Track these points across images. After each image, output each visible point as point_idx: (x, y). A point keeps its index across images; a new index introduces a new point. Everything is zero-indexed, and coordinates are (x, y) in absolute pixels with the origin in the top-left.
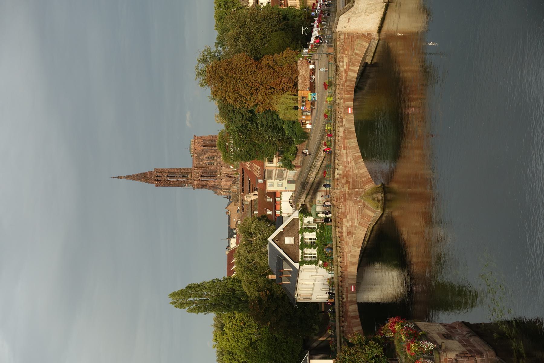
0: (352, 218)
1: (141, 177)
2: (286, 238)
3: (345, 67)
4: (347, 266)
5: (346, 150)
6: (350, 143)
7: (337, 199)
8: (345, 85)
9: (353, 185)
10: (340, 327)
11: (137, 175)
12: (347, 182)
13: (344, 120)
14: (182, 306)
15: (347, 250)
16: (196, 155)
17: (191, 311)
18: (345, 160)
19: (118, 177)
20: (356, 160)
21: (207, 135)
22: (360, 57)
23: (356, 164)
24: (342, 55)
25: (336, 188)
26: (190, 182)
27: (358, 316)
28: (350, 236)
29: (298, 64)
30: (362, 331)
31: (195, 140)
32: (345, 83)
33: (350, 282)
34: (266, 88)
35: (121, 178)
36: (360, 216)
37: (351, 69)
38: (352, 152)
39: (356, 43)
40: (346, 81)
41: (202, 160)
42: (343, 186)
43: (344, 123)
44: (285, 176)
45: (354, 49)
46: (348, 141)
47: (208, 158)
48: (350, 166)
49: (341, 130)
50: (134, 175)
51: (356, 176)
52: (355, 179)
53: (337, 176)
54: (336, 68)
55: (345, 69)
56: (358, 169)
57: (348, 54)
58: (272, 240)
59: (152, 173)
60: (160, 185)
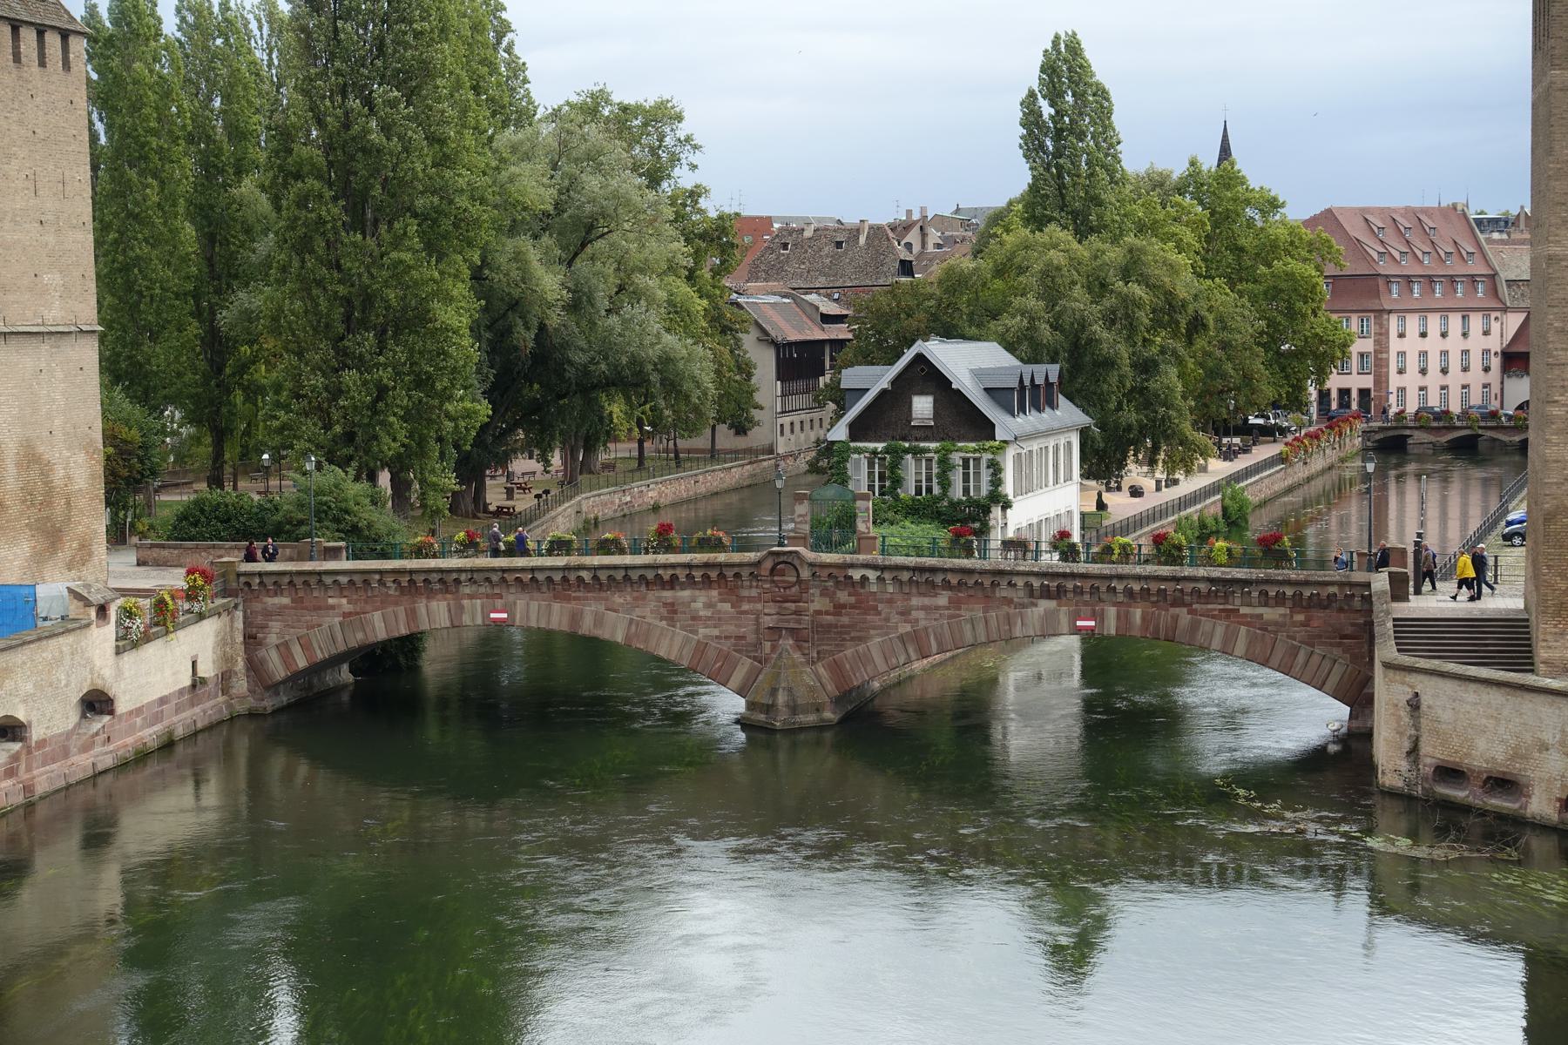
0: (720, 619)
3: (1244, 610)
4: (568, 599)
6: (972, 621)
9: (830, 626)
10: (381, 572)
12: (839, 608)
13: (1052, 604)
14: (1049, 69)
15: (618, 599)
23: (901, 638)
27: (415, 630)
28: (664, 611)
30: (372, 639)
33: (520, 604)
36: (726, 646)
39: (1337, 652)
48: (895, 618)
52: (849, 633)
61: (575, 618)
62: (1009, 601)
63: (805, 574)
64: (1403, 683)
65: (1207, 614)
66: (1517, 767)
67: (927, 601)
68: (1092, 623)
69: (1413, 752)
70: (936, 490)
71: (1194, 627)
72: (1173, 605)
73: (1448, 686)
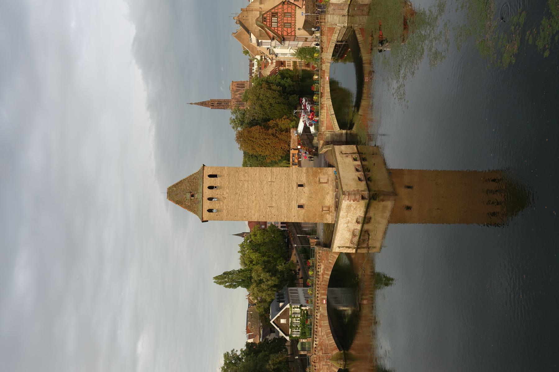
1: (203, 104)
2: (281, 320)
3: (322, 272)
5: (321, 329)
7: (315, 360)
8: (322, 284)
9: (325, 351)
11: (201, 102)
12: (321, 349)
13: (320, 308)
14: (220, 283)
16: (233, 92)
17: (226, 287)
18: (320, 334)
19: (190, 104)
21: (239, 81)
22: (332, 265)
24: (320, 263)
25: (314, 354)
26: (230, 107)
29: (291, 132)
31: (232, 83)
32: (322, 283)
34: (271, 146)
35: (192, 104)
37: (326, 273)
38: (325, 329)
39: (330, 255)
40: (322, 281)
41: (236, 95)
42: (319, 352)
43: (320, 310)
45: (328, 259)
46: (323, 322)
48: (323, 338)
49: (318, 314)
50: (199, 103)
51: (327, 345)
53: (315, 346)
54: (316, 273)
55: (322, 273)
56: (328, 340)
57: (324, 263)
58: (273, 322)
59: (209, 102)
60: (213, 108)
64: (336, 249)
68: (324, 300)
69: (349, 247)
70: (299, 319)
71: (325, 281)
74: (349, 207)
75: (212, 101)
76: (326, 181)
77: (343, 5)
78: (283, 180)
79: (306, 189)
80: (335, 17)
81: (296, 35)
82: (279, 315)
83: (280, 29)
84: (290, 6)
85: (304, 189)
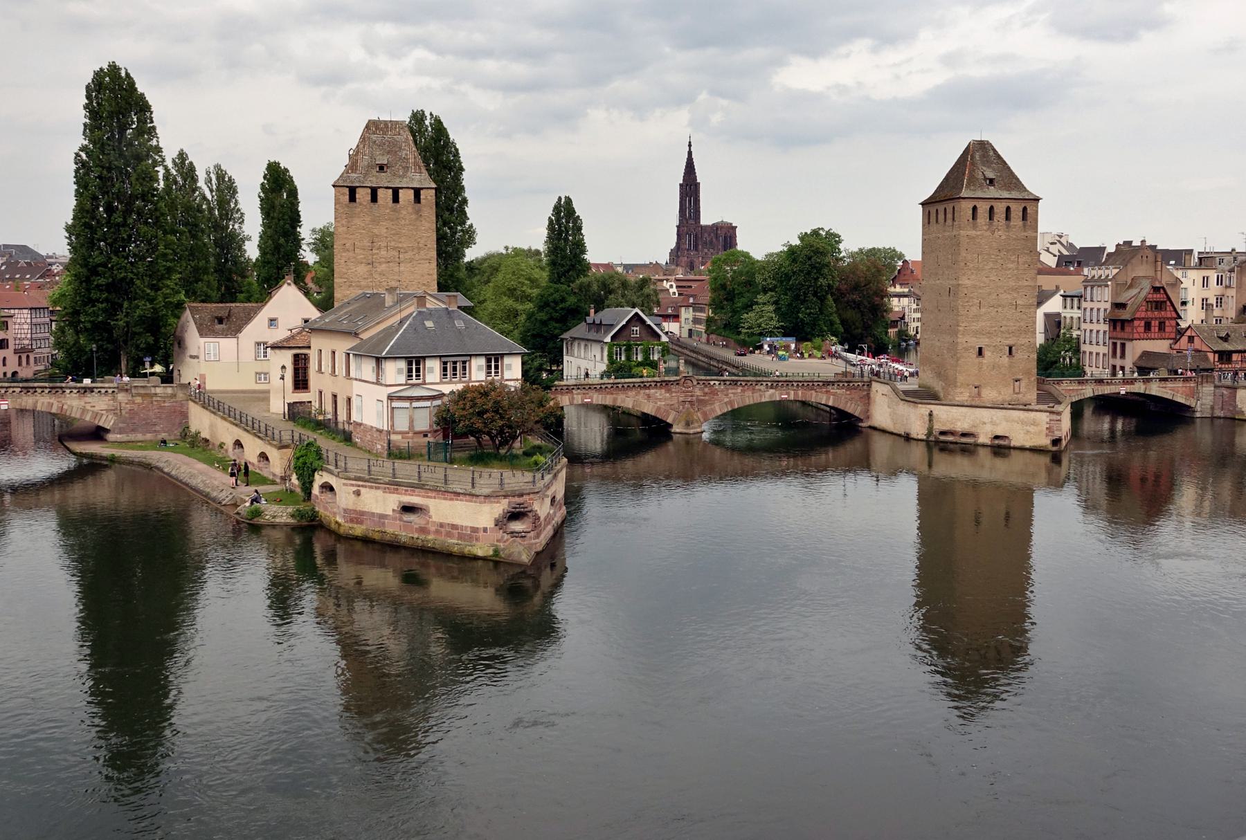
4: (612, 394)
12: (705, 394)
19: (690, 142)
20: (731, 403)
28: (646, 397)
35: (690, 145)
36: (668, 408)
44: (697, 326)
47: (711, 242)
53: (712, 383)
58: (636, 314)
61: (615, 400)
62: (760, 390)
63: (695, 383)
65: (821, 392)
66: (973, 430)
67: (733, 391)
72: (812, 390)
73: (945, 407)
74: (1034, 423)
75: (697, 185)
76: (1017, 390)
77: (1231, 409)
78: (1018, 324)
79: (1005, 359)
80: (1211, 398)
81: (1134, 341)
82: (649, 322)
83: (1143, 316)
84: (1174, 330)
85: (1005, 356)
